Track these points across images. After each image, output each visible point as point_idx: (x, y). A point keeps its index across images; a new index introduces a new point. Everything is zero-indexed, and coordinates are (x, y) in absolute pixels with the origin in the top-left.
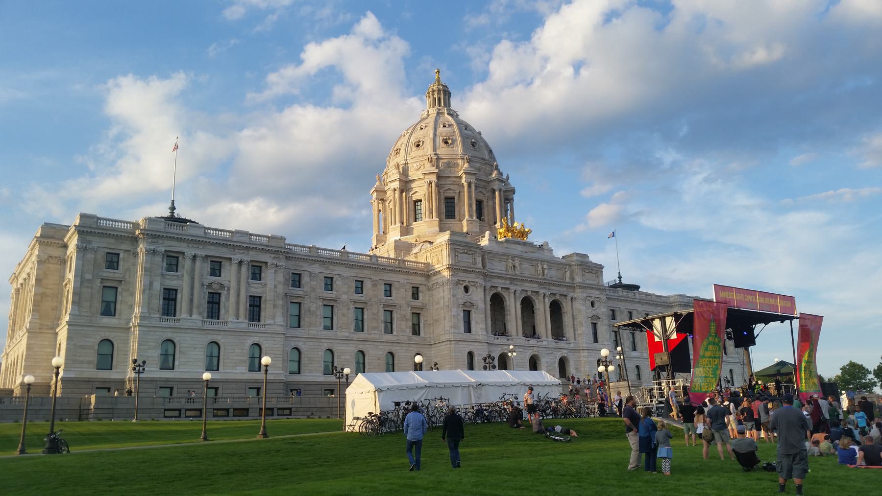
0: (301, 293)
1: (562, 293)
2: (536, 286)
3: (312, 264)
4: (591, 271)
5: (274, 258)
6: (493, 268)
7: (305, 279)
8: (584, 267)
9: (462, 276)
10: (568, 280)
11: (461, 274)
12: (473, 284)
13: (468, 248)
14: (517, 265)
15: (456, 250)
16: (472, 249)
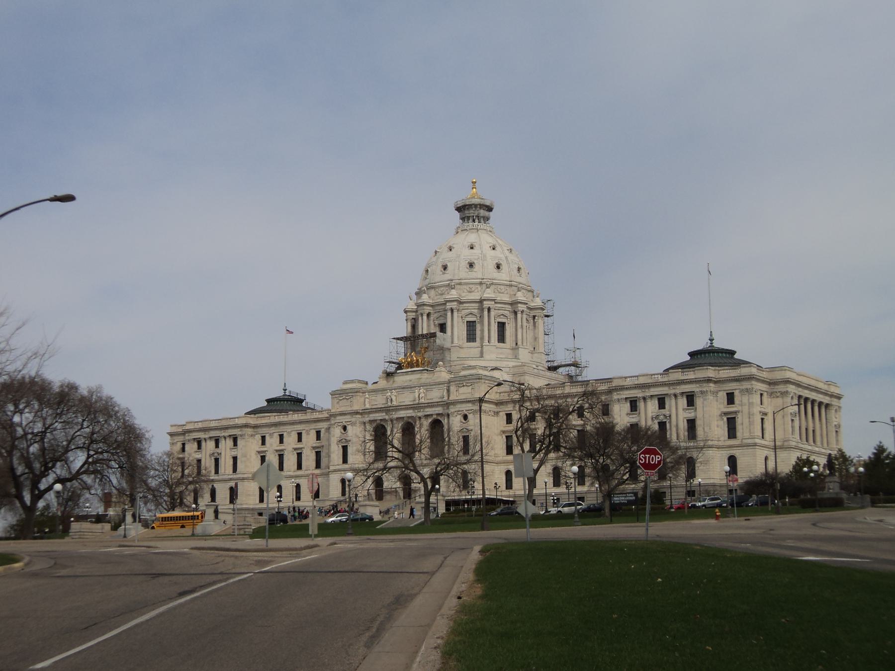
0: (265, 449)
1: (437, 412)
2: (411, 411)
3: (270, 428)
4: (464, 384)
5: (241, 431)
6: (376, 403)
7: (267, 438)
8: (457, 383)
9: (340, 419)
10: (446, 398)
11: (338, 418)
12: (348, 423)
13: (346, 395)
14: (394, 398)
15: (338, 398)
16: (349, 394)
